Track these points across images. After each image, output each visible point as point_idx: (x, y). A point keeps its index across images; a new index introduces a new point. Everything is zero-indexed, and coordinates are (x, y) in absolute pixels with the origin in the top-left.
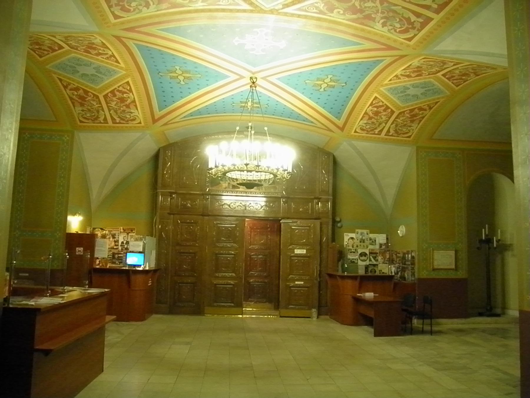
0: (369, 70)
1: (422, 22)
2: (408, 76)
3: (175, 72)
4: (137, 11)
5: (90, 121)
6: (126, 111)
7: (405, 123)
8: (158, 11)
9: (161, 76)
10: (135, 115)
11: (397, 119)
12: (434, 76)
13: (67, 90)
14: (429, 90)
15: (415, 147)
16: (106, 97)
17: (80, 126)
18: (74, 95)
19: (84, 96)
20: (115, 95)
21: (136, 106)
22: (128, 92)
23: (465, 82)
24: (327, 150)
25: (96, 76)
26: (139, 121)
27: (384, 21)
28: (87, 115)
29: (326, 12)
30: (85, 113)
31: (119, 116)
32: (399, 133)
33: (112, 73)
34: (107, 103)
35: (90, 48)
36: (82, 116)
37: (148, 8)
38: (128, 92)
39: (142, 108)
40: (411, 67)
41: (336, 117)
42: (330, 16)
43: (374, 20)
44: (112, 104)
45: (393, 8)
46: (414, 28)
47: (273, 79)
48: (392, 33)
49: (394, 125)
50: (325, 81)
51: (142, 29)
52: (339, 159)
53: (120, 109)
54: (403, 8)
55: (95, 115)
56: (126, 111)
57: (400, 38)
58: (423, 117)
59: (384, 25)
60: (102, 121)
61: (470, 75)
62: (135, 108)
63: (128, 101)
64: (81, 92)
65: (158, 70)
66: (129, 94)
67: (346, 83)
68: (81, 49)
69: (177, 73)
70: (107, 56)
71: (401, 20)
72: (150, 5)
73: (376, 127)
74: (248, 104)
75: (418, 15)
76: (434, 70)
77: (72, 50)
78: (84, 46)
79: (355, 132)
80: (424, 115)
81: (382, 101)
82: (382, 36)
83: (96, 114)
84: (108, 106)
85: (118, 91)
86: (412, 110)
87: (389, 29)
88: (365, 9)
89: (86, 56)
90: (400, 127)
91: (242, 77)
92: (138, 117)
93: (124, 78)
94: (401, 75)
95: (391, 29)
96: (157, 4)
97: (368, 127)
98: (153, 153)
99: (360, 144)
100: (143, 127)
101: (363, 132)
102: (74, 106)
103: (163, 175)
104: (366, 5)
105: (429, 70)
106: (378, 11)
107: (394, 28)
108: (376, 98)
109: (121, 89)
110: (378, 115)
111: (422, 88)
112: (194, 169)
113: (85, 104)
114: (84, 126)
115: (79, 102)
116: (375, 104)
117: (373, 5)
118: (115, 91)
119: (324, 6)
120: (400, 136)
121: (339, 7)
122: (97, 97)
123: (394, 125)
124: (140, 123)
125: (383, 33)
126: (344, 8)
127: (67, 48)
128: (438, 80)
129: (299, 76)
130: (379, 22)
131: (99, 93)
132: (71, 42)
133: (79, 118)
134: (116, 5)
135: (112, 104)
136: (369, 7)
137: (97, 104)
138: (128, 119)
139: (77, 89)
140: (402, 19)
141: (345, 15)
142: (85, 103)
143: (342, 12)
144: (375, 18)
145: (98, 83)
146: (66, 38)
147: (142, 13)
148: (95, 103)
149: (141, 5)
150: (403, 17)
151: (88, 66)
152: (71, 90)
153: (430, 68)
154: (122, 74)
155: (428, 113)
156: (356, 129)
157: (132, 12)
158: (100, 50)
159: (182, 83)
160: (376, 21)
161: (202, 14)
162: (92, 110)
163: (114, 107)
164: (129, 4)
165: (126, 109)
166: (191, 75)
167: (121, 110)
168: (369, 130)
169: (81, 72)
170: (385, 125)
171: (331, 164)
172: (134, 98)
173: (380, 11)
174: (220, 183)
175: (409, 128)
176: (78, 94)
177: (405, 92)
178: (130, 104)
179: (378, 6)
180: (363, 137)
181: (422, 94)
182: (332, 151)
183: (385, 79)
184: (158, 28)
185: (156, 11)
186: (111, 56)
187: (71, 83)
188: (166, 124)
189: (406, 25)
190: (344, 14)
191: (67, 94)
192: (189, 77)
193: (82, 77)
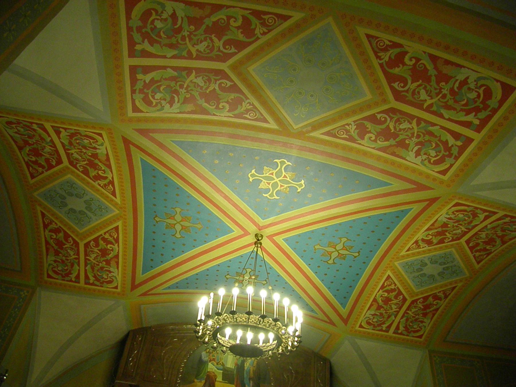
0: (389, 229)
2: (429, 242)
3: (173, 218)
4: (159, 107)
5: (60, 277)
6: (105, 269)
7: (417, 317)
8: (180, 113)
9: (157, 222)
10: (113, 276)
11: (408, 310)
12: (458, 244)
13: (46, 230)
14: (448, 268)
15: (427, 352)
16: (87, 245)
17: (46, 282)
18: (52, 238)
20: (97, 245)
22: (114, 241)
23: (488, 255)
24: (324, 355)
25: (85, 213)
26: (116, 285)
27: (419, 148)
30: (57, 265)
31: (95, 274)
32: (409, 331)
33: (103, 210)
34: (86, 254)
36: (52, 268)
37: (171, 106)
38: (114, 241)
39: (124, 270)
40: (436, 225)
41: (341, 304)
42: (360, 144)
47: (279, 239)
49: (404, 319)
50: (337, 248)
51: (156, 136)
52: (336, 368)
53: (99, 265)
55: (67, 270)
56: (105, 269)
57: (434, 171)
58: (437, 310)
59: (418, 154)
60: (74, 279)
61: (496, 242)
63: (110, 256)
65: (155, 212)
66: (114, 245)
67: (359, 252)
69: (175, 220)
71: (437, 145)
72: (174, 102)
73: (385, 321)
74: (244, 277)
76: (459, 231)
79: (361, 326)
80: (438, 306)
81: (394, 283)
82: (414, 171)
83: (69, 268)
84: (86, 259)
85: (104, 240)
86: (426, 298)
88: (399, 133)
90: (411, 322)
91: (246, 233)
92: (116, 278)
93: (115, 221)
94: (423, 240)
97: (375, 320)
98: (120, 336)
99: (364, 344)
100: (119, 294)
101: (369, 327)
103: (127, 362)
105: (454, 232)
106: (413, 134)
108: (389, 277)
109: (107, 236)
110: (388, 303)
111: (440, 264)
112: (165, 360)
113: (61, 253)
116: (386, 286)
117: (410, 126)
120: (411, 335)
123: (404, 319)
124: (116, 288)
128: (460, 249)
129: (310, 238)
130: (412, 151)
134: (141, 91)
135: (91, 257)
136: (404, 129)
137: (74, 255)
138: (103, 280)
139: (57, 231)
141: (376, 142)
142: (62, 251)
143: (373, 138)
144: (409, 144)
148: (72, 253)
150: (440, 140)
153: (457, 226)
154: (114, 214)
155: (443, 304)
156: (361, 322)
157: (153, 107)
159: (178, 235)
160: (409, 149)
161: (225, 130)
163: (92, 260)
164: (153, 94)
165: (106, 266)
166: (190, 225)
167: (99, 267)
168: (376, 324)
169: (69, 207)
170: (394, 319)
171: (328, 375)
172: (118, 252)
173: (415, 135)
174: (194, 382)
175: (421, 325)
177: (422, 270)
178: (111, 259)
179: (414, 127)
180: (369, 333)
181: (439, 274)
182: (328, 356)
183: (400, 250)
184: (173, 140)
185: (178, 113)
187: (53, 221)
188: (145, 294)
190: (375, 141)
191: (45, 236)
192: (187, 227)
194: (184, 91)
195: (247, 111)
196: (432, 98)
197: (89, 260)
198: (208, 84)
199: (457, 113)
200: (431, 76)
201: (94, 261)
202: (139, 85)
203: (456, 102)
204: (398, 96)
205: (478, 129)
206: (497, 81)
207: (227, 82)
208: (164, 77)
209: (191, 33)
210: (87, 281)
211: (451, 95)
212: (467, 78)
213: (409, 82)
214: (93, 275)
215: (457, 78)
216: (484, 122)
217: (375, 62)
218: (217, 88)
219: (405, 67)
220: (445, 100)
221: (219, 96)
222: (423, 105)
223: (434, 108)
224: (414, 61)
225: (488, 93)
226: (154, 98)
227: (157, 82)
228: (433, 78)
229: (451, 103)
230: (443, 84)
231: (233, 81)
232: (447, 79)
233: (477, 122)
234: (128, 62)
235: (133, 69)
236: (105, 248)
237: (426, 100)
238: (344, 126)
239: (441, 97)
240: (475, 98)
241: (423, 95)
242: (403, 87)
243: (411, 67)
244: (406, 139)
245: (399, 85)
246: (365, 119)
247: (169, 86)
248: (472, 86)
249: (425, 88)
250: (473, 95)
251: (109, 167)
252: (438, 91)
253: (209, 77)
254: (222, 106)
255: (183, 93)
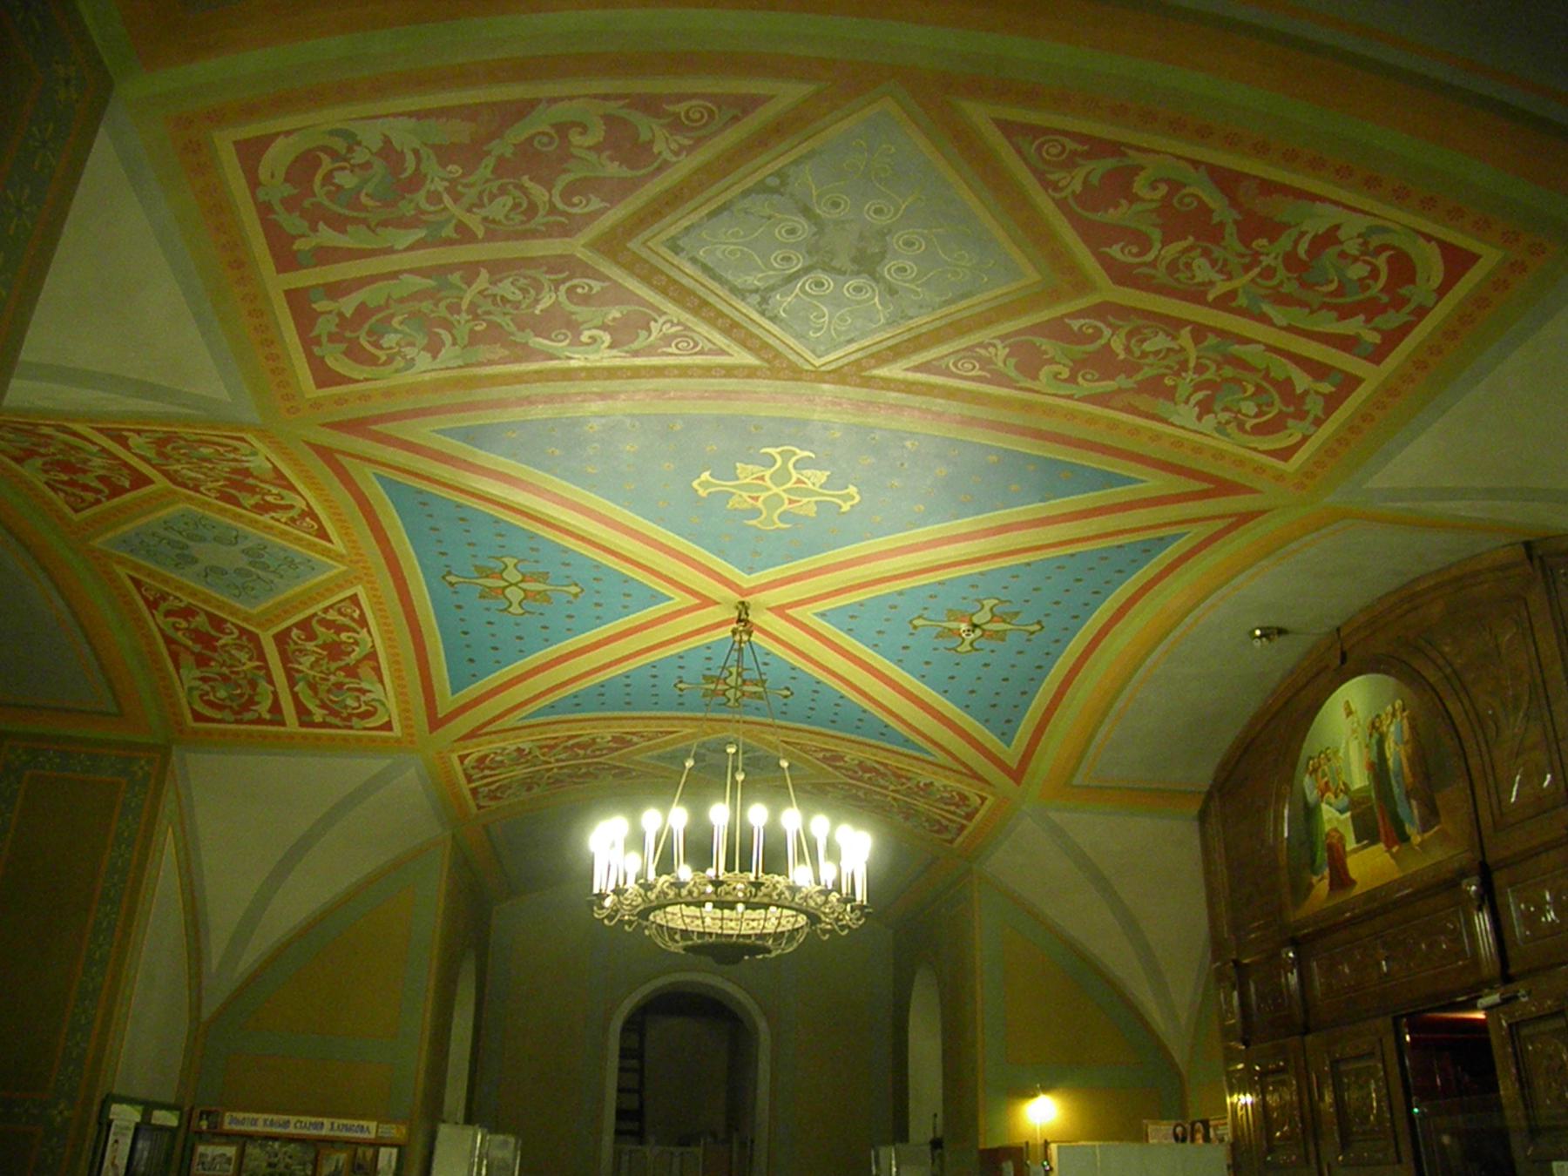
1: (1331, 394)
4: (399, 363)
5: (227, 715)
8: (467, 366)
10: (373, 700)
16: (281, 639)
17: (195, 732)
18: (177, 629)
19: (208, 634)
20: (311, 636)
21: (377, 670)
22: (353, 625)
26: (386, 719)
28: (218, 695)
29: (1013, 373)
30: (213, 688)
31: (321, 700)
34: (285, 659)
35: (239, 484)
38: (353, 625)
39: (398, 677)
43: (1169, 394)
44: (300, 664)
45: (1236, 349)
46: (1301, 415)
48: (1228, 435)
53: (328, 680)
54: (1271, 349)
55: (241, 695)
60: (268, 716)
62: (375, 678)
63: (353, 656)
64: (200, 621)
68: (209, 490)
70: (293, 513)
75: (1318, 370)
77: (179, 489)
78: (217, 481)
83: (248, 691)
85: (323, 622)
87: (1219, 423)
88: (1142, 361)
89: (222, 511)
92: (383, 704)
95: (1228, 422)
96: (466, 342)
100: (398, 741)
102: (177, 667)
104: (1147, 347)
107: (1236, 418)
114: (209, 733)
115: (193, 653)
117: (1169, 344)
118: (314, 623)
119: (1008, 356)
121: (1057, 359)
122: (254, 638)
124: (388, 726)
125: (1197, 437)
126: (1074, 361)
127: (161, 483)
131: (259, 625)
132: (178, 467)
133: (189, 703)
135: (300, 664)
138: (349, 711)
139: (188, 613)
140: (1265, 384)
142: (216, 655)
145: (255, 597)
146: (161, 443)
147: (413, 370)
148: (243, 656)
149: (412, 344)
151: (231, 544)
152: (168, 614)
157: (383, 364)
158: (269, 493)
162: (233, 676)
164: (374, 338)
165: (347, 680)
172: (373, 646)
176: (193, 626)
178: (359, 662)
185: (460, 367)
186: (303, 515)
187: (168, 594)
189: (1278, 405)
193: (206, 576)
194: (464, 317)
195: (667, 339)
196: (1230, 277)
197: (298, 671)
198: (533, 292)
199: (1312, 312)
200: (1222, 224)
201: (312, 673)
202: (324, 327)
203: (1303, 284)
204: (1122, 275)
205: (1377, 356)
206: (1429, 238)
207: (592, 283)
208: (395, 296)
209: (453, 182)
210: (305, 718)
211: (1288, 268)
212: (1337, 227)
213: (1157, 245)
214: (318, 702)
215: (1304, 228)
216: (1392, 339)
217: (1044, 202)
218: (563, 297)
219: (1138, 207)
220: (1275, 282)
221: (574, 317)
222: (1205, 293)
223: (1242, 301)
224: (1163, 189)
225: (1403, 269)
226: (380, 347)
227: (379, 309)
228: (1230, 229)
229: (1290, 288)
230: (1262, 242)
231: (607, 278)
232: (1273, 230)
233: (1376, 338)
234: (276, 284)
235: (298, 301)
236: (334, 641)
237: (1211, 283)
238: (970, 349)
239: (1260, 275)
240: (1367, 278)
241: (1203, 271)
242: (1140, 254)
243: (1154, 205)
244: (1162, 377)
245: (1126, 251)
246: (1034, 330)
247: (413, 315)
248: (1352, 248)
249: (1206, 253)
250: (1357, 271)
251: (292, 488)
252: (1247, 260)
253: (535, 279)
254: (590, 337)
255: (463, 322)
